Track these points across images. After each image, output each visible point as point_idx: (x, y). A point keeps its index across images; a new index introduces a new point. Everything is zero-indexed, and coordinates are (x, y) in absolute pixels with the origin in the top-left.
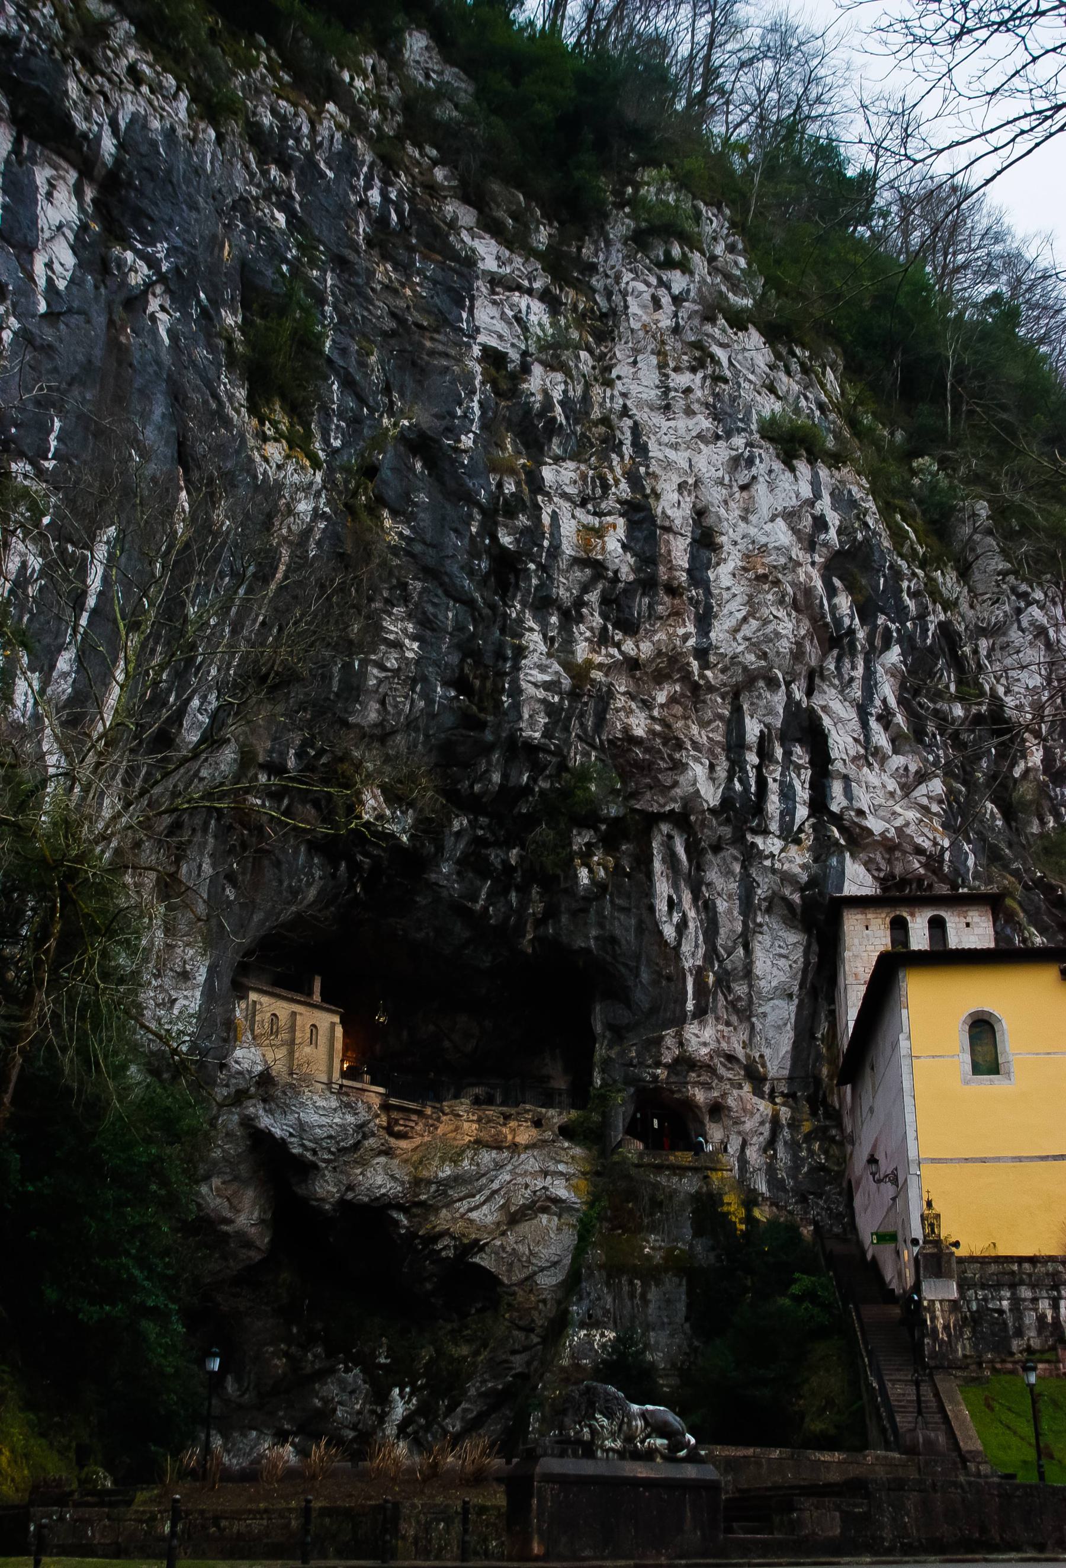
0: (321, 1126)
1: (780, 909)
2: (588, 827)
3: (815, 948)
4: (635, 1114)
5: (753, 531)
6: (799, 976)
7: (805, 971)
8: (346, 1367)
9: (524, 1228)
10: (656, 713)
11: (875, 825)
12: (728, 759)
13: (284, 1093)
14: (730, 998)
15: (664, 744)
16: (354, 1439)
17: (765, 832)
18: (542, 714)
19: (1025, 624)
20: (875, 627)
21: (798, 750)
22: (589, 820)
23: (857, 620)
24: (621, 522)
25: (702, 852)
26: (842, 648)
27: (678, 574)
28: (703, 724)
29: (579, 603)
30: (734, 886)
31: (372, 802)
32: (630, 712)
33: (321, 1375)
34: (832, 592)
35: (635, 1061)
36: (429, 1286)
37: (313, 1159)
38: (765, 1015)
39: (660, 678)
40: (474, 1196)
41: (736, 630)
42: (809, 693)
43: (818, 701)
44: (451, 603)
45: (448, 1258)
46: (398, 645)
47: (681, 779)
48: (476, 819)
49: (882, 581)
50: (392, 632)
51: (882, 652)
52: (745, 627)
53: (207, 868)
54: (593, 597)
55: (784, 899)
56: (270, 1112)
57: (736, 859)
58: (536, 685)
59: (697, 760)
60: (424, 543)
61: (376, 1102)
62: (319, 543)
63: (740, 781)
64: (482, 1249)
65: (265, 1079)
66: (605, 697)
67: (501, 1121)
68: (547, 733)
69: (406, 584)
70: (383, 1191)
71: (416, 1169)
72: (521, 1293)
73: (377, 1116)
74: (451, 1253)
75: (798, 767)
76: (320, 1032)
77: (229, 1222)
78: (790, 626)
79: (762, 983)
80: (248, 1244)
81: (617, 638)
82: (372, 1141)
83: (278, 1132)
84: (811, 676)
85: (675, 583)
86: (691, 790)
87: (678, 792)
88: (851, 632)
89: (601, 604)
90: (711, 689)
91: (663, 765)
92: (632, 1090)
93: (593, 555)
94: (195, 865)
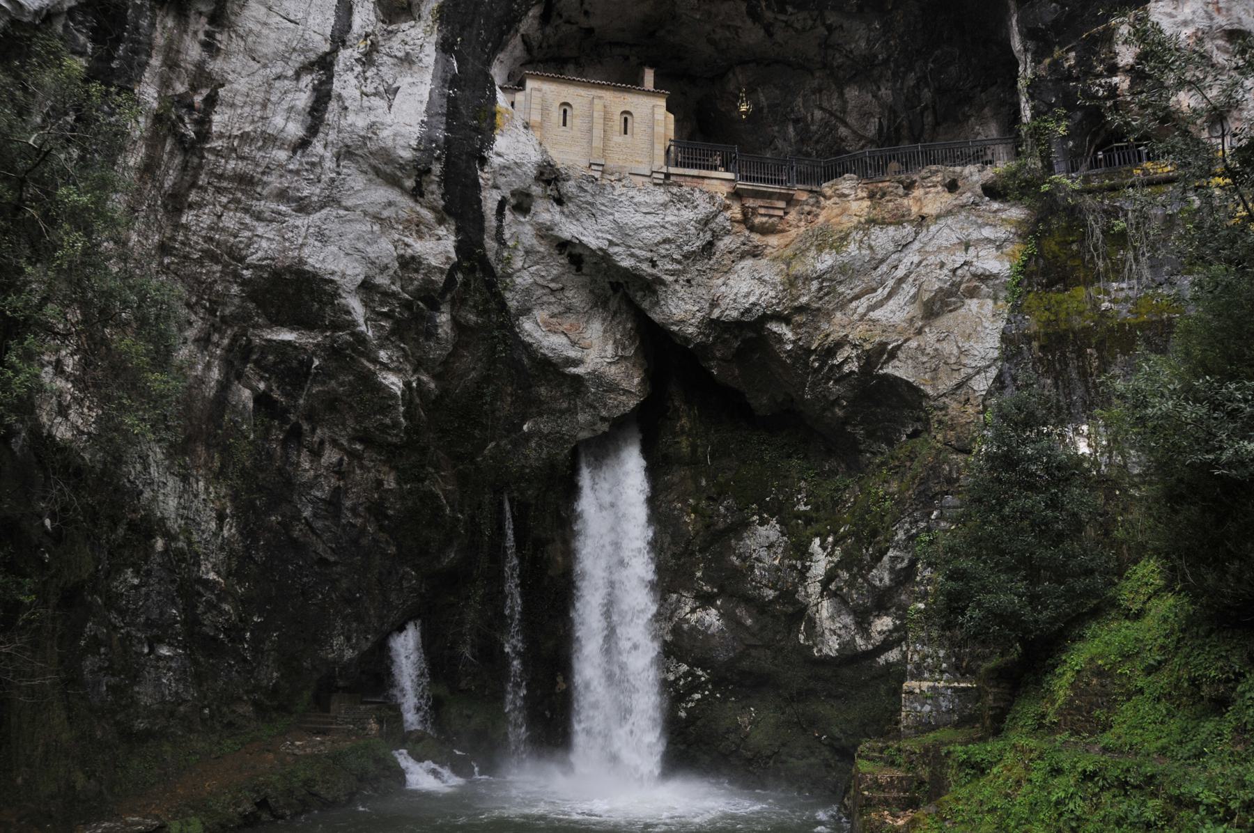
8: (761, 518)
9: (946, 321)
16: (777, 598)
37: (655, 271)
40: (874, 290)
45: (852, 372)
56: (572, 215)
61: (722, 190)
64: (893, 355)
67: (901, 191)
70: (752, 299)
71: (788, 265)
72: (954, 405)
73: (728, 208)
74: (854, 366)
76: (636, 120)
77: (577, 363)
80: (613, 388)
83: (592, 242)
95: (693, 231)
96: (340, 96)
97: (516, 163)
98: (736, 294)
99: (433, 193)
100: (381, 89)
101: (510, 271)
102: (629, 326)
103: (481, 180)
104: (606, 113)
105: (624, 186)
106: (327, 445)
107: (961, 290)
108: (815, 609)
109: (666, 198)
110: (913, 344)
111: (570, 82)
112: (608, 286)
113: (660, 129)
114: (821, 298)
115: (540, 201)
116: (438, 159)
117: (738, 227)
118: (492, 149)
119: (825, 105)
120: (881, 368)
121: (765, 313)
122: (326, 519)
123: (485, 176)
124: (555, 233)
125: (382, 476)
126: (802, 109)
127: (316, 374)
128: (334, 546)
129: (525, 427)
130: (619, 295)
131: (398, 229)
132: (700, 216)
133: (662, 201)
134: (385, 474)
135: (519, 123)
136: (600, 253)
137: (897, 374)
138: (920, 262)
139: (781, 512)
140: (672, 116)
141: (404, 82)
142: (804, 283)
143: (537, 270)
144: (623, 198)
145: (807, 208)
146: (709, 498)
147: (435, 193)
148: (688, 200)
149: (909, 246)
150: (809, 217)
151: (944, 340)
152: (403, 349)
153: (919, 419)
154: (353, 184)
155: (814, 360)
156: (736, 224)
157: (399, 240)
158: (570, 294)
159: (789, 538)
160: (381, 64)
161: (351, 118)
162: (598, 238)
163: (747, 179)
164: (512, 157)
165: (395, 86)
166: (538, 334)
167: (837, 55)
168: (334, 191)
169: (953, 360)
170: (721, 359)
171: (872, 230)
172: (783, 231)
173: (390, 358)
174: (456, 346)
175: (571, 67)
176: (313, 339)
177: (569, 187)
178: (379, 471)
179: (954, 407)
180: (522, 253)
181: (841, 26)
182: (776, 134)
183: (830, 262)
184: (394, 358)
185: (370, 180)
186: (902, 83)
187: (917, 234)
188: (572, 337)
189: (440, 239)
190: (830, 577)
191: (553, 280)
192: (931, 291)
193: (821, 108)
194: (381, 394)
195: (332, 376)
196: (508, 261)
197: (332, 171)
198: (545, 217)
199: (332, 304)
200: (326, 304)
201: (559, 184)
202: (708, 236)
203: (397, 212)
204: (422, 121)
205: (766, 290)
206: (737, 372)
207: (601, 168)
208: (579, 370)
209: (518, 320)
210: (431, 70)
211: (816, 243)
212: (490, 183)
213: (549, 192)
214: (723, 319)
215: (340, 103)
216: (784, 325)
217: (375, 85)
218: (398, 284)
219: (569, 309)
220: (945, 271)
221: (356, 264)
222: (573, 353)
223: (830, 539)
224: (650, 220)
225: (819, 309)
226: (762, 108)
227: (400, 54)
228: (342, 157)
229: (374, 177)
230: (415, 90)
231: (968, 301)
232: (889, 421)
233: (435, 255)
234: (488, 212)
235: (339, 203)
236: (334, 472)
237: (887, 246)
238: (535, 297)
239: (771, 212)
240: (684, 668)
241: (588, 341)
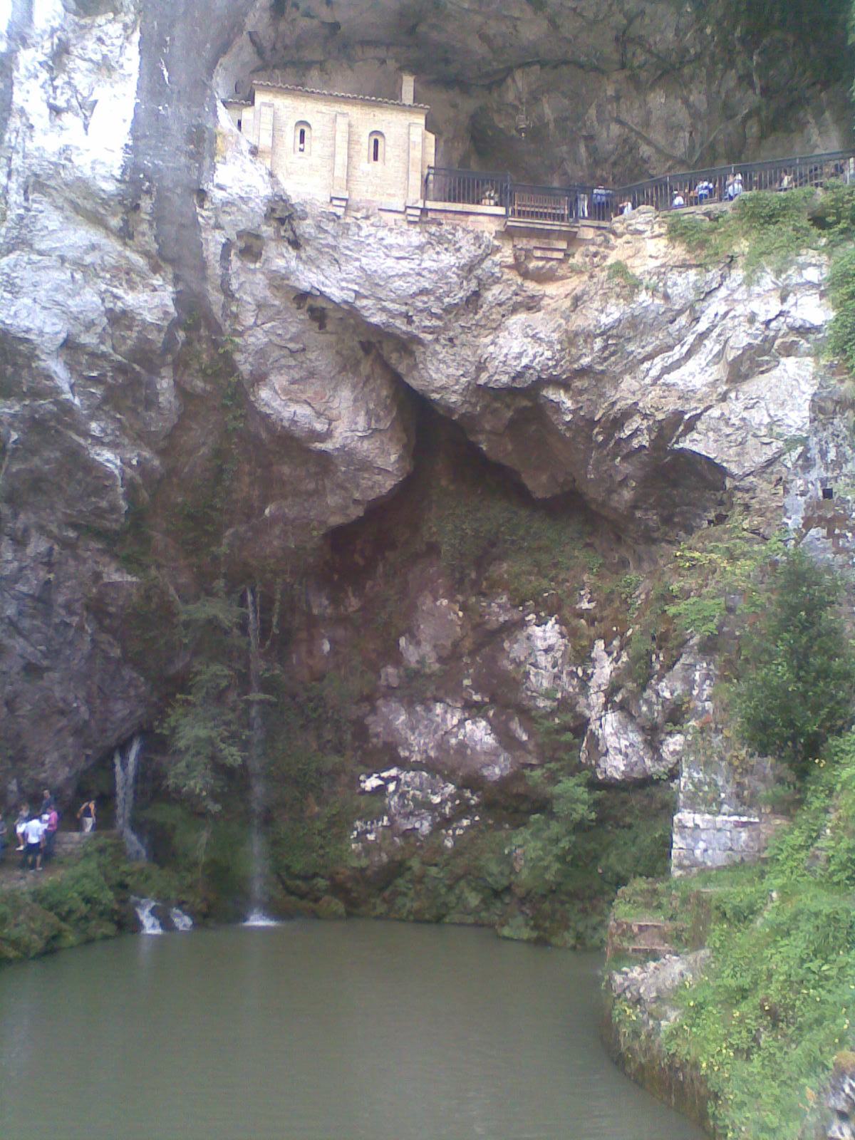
8: (538, 616)
9: (757, 385)
13: (319, 228)
36: (627, 494)
37: (409, 329)
40: (671, 348)
56: (310, 261)
61: (489, 228)
64: (690, 427)
70: (525, 361)
71: (567, 319)
72: (764, 485)
73: (497, 249)
74: (644, 440)
80: (366, 466)
82: (496, 289)
83: (336, 293)
95: (455, 277)
96: (22, 112)
97: (241, 198)
98: (506, 355)
99: (144, 234)
100: (74, 102)
101: (240, 328)
102: (384, 393)
103: (200, 219)
104: (350, 134)
105: (372, 225)
106: (33, 532)
107: (775, 346)
108: (598, 723)
109: (423, 239)
110: (715, 412)
111: (309, 95)
112: (358, 346)
113: (416, 154)
114: (606, 359)
115: (273, 244)
116: (148, 192)
117: (510, 275)
118: (213, 181)
119: (625, 117)
120: (677, 442)
121: (539, 377)
122: (33, 617)
123: (205, 213)
124: (291, 283)
125: (101, 568)
126: (595, 123)
127: (15, 450)
128: (42, 648)
129: (267, 511)
130: (372, 357)
131: (104, 278)
132: (463, 261)
133: (417, 243)
134: (104, 566)
135: (245, 147)
136: (346, 307)
137: (695, 448)
138: (726, 313)
140: (432, 137)
141: (103, 93)
142: (585, 341)
143: (273, 327)
144: (371, 240)
145: (593, 249)
146: (484, 595)
147: (146, 235)
148: (449, 241)
149: (713, 294)
150: (596, 260)
151: (752, 407)
152: (119, 420)
153: (721, 503)
154: (47, 223)
155: (598, 433)
156: (506, 270)
157: (106, 291)
158: (312, 356)
159: (569, 641)
160: (73, 70)
162: (342, 289)
164: (235, 191)
165: (92, 99)
166: (276, 404)
167: (639, 51)
168: (24, 231)
170: (491, 432)
171: (669, 275)
172: (563, 278)
173: (103, 430)
174: (182, 417)
176: (10, 408)
177: (306, 227)
178: (97, 563)
179: (764, 487)
180: (254, 307)
181: (643, 13)
182: (566, 156)
183: (616, 315)
184: (109, 431)
185: (67, 218)
186: (720, 85)
187: (723, 277)
188: (317, 407)
189: (155, 290)
190: (613, 689)
191: (291, 340)
192: (738, 349)
193: (620, 122)
194: (94, 473)
195: (33, 452)
197: (19, 206)
198: (281, 263)
199: (30, 367)
200: (22, 367)
201: (295, 223)
202: (473, 285)
203: (102, 258)
204: (127, 145)
205: (540, 350)
206: (510, 447)
207: (344, 204)
208: (328, 446)
209: (253, 386)
210: (136, 76)
211: (601, 292)
212: (212, 222)
213: (283, 233)
214: (491, 385)
215: (24, 119)
216: (562, 392)
217: (66, 97)
218: (109, 343)
219: (312, 374)
220: (757, 325)
221: (55, 320)
222: (320, 426)
224: (404, 266)
225: (603, 372)
226: (547, 124)
227: (98, 57)
228: (30, 189)
229: (73, 215)
231: (783, 360)
232: (686, 505)
233: (150, 310)
234: (211, 257)
235: (31, 246)
236: (42, 563)
237: (687, 293)
238: (271, 360)
239: (549, 254)
240: (451, 788)
241: (335, 412)
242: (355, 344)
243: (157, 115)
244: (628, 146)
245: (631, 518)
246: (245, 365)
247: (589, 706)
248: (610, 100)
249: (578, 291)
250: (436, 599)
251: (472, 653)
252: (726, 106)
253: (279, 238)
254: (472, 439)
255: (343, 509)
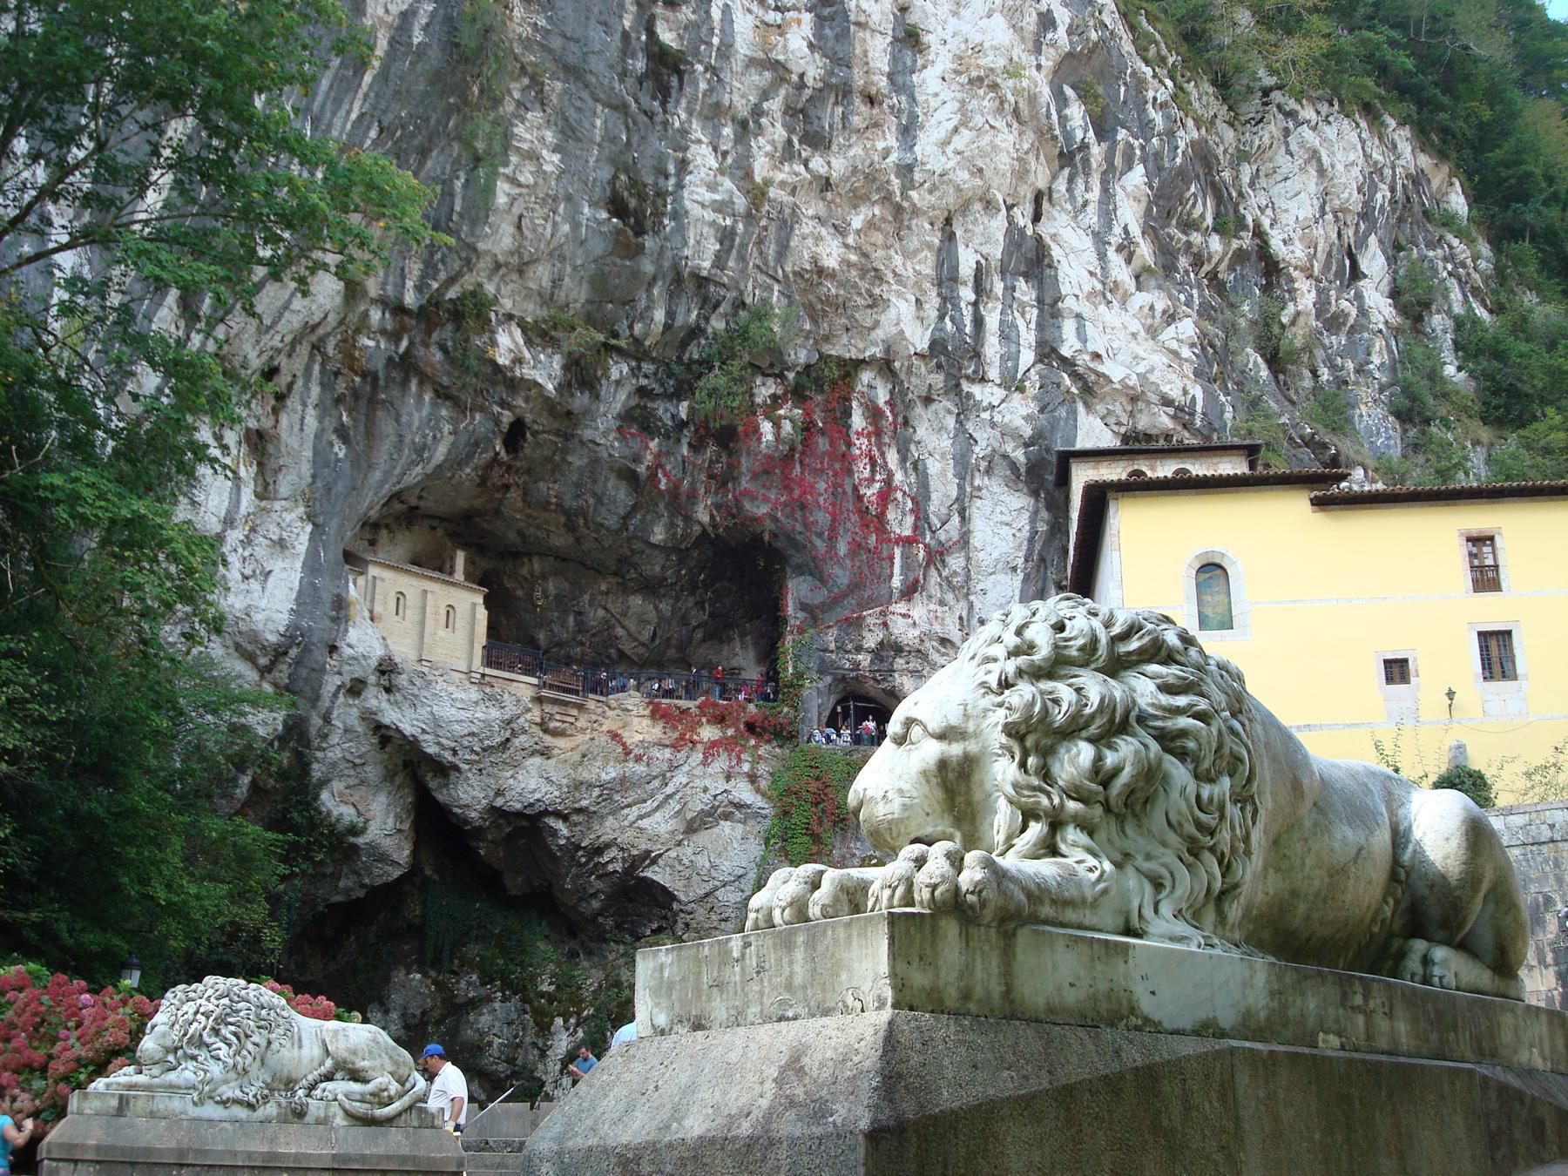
0: (459, 722)
1: (1002, 470)
2: (776, 376)
3: (1044, 514)
4: (835, 708)
5: (965, 28)
6: (1024, 547)
7: (1031, 540)
9: (702, 838)
10: (850, 240)
11: (1115, 371)
12: (939, 294)
14: (944, 574)
15: (862, 278)
17: (983, 380)
18: (712, 240)
19: (1294, 147)
20: (1114, 143)
21: (1021, 284)
22: (773, 365)
23: (1091, 133)
24: (807, 18)
25: (909, 405)
26: (1074, 166)
27: (875, 78)
28: (907, 255)
29: (757, 112)
30: (946, 443)
31: (507, 343)
32: (818, 239)
33: (474, 1004)
34: (1062, 101)
35: (832, 646)
36: (596, 904)
38: (984, 592)
39: (857, 199)
40: (645, 801)
41: (945, 143)
42: (1037, 218)
43: (1045, 229)
44: (599, 108)
46: (533, 156)
47: (883, 318)
48: (639, 368)
49: (1122, 89)
50: (525, 140)
51: (1122, 174)
52: (956, 138)
53: (311, 422)
54: (775, 105)
55: (1005, 456)
56: (396, 702)
57: (949, 412)
58: (703, 206)
59: (900, 295)
60: (565, 37)
62: (426, 28)
63: (952, 320)
64: (654, 862)
65: (387, 669)
66: (787, 223)
68: (719, 262)
69: (542, 84)
70: (538, 796)
72: (701, 910)
73: (529, 710)
75: (1023, 305)
78: (1011, 138)
79: (981, 555)
80: (383, 858)
81: (804, 154)
82: (523, 738)
83: (408, 729)
84: (1038, 198)
85: (873, 91)
86: (894, 330)
87: (879, 334)
88: (1084, 146)
89: (785, 113)
90: (916, 212)
91: (860, 301)
92: (829, 679)
93: (773, 55)
94: (297, 417)
110: (673, 854)
117: (536, 729)
119: (610, 606)
135: (367, 614)
139: (519, 989)
141: (277, 565)
145: (594, 717)
146: (455, 973)
153: (665, 918)
158: (368, 769)
161: (231, 599)
163: (551, 687)
169: (704, 872)
175: (384, 532)
177: (402, 680)
179: (701, 912)
196: (325, 737)
198: (373, 703)
202: (508, 734)
208: (360, 841)
219: (362, 783)
223: (572, 1021)
227: (275, 538)
230: (284, 575)
242: (400, 762)
243: (313, 585)
244: (608, 625)
245: (593, 921)
246: (317, 771)
247: (546, 1073)
248: (601, 593)
249: (583, 748)
250: (409, 973)
251: (438, 1023)
252: (683, 617)
253: (378, 685)
254: (473, 844)
255: (347, 891)
